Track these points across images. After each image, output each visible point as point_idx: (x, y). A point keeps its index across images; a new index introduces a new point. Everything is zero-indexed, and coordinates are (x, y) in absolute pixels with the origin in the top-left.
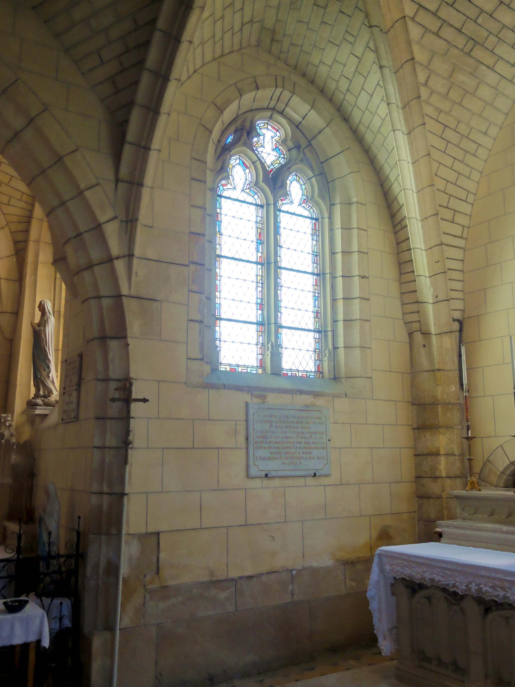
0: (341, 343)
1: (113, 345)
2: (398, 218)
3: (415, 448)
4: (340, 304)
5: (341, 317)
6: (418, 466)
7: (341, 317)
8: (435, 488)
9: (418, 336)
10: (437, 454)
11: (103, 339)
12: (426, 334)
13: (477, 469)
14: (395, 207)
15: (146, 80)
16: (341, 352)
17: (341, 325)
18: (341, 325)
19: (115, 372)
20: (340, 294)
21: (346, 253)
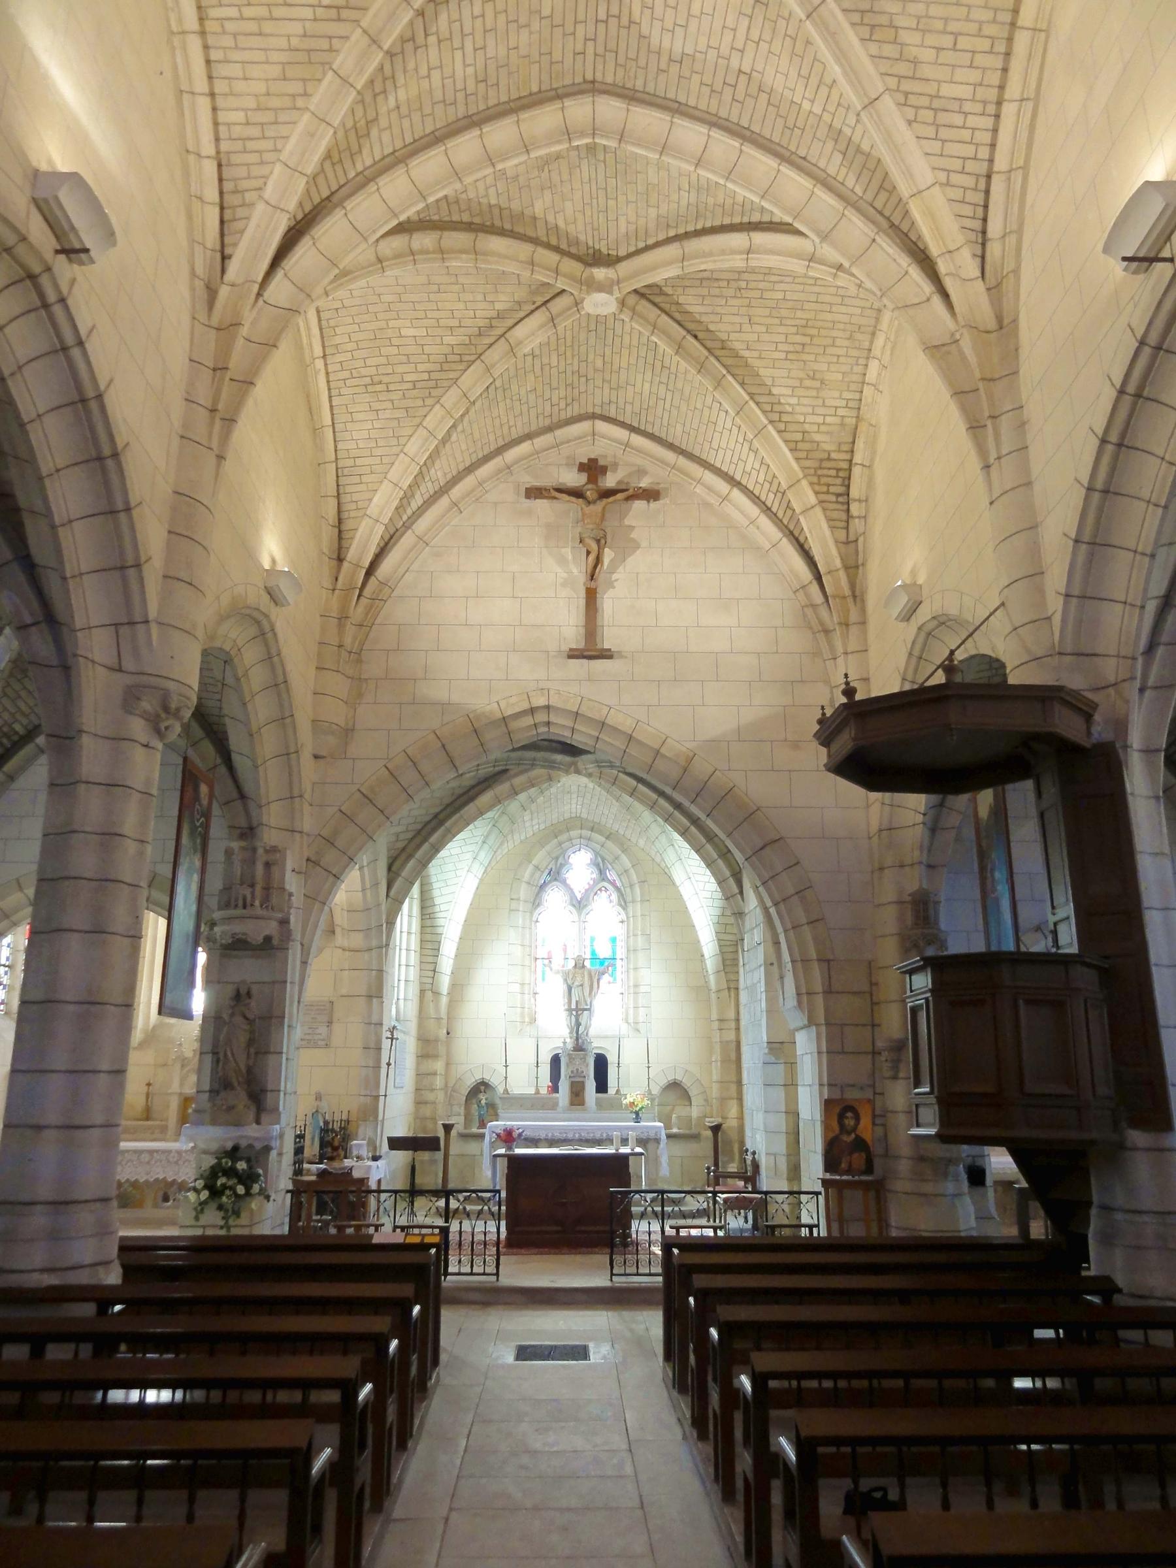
0: (402, 996)
1: (375, 1000)
2: (429, 911)
3: (417, 1069)
4: (403, 968)
5: (403, 978)
6: (417, 1082)
7: (403, 978)
8: (430, 1096)
9: (429, 994)
10: (435, 1074)
11: (370, 997)
12: (436, 994)
13: (451, 1084)
14: (428, 903)
15: (426, 846)
16: (401, 1002)
17: (402, 984)
18: (402, 984)
19: (375, 1019)
20: (403, 962)
21: (409, 933)
